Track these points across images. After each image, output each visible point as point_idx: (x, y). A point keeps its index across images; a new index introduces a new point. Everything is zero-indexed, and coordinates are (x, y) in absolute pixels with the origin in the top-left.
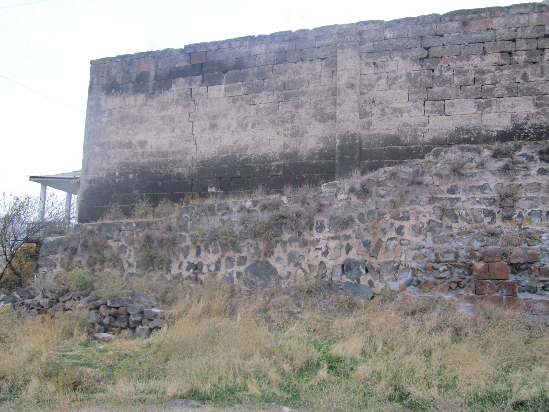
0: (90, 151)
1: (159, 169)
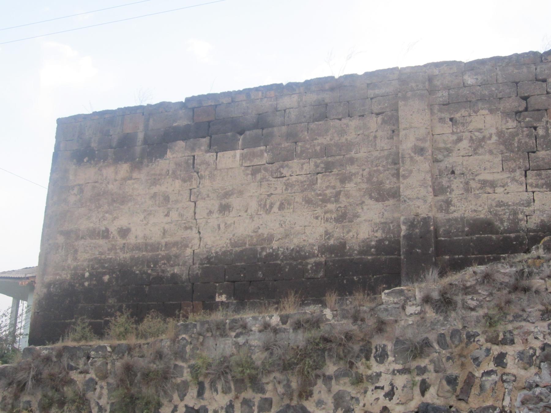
1: (145, 268)
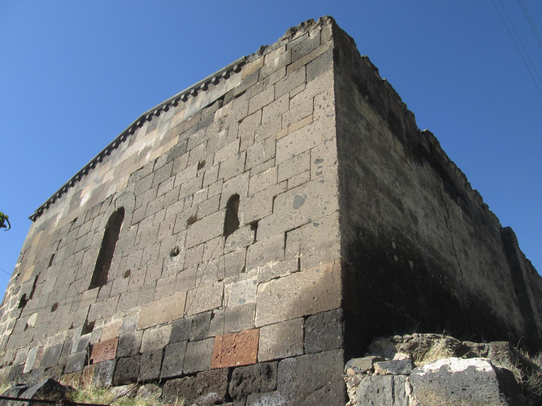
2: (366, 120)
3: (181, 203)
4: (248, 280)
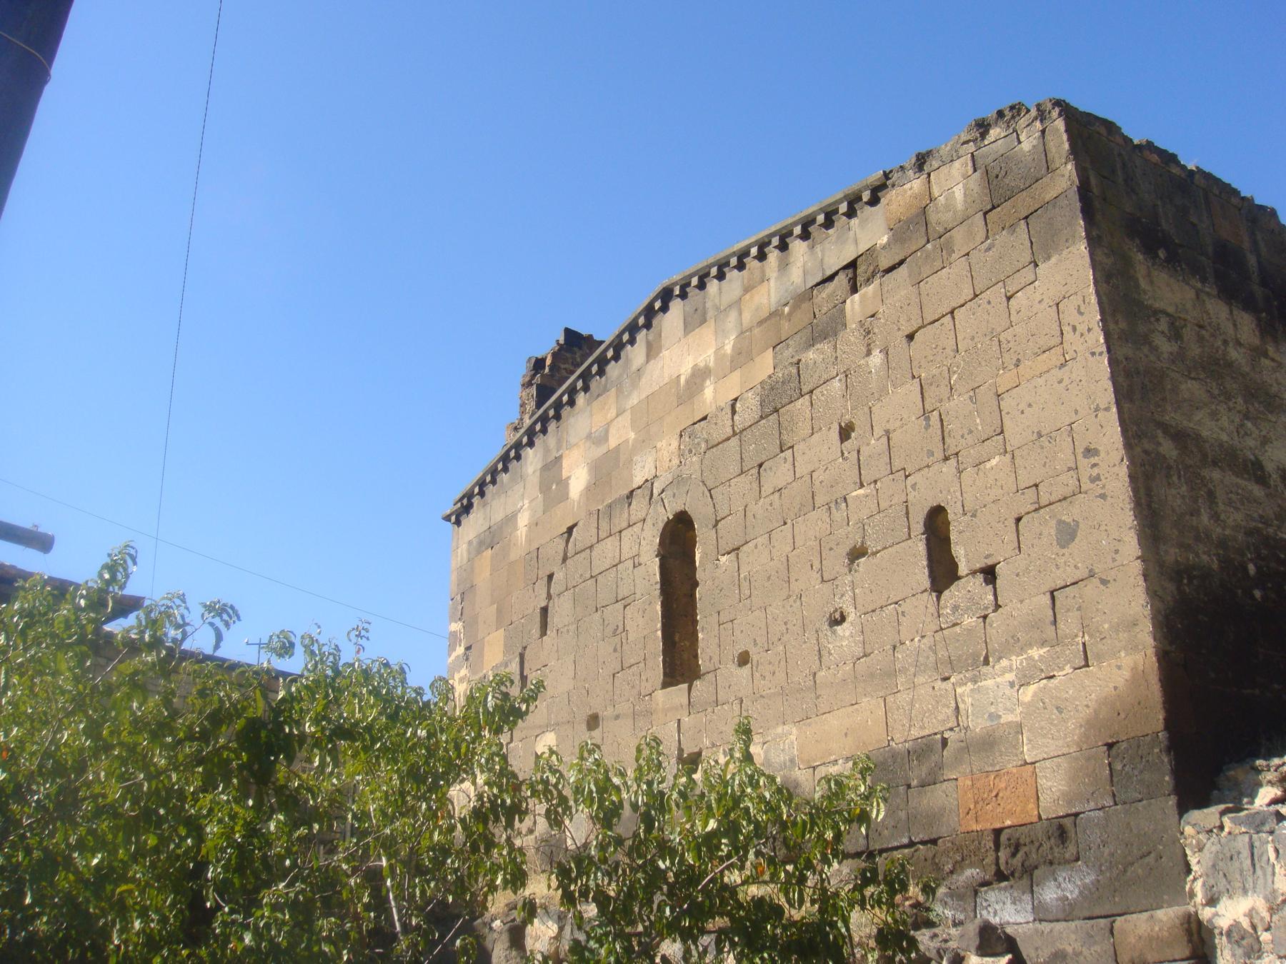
0: (1147, 446)
2: (1168, 315)
3: (821, 513)
4: (998, 680)
